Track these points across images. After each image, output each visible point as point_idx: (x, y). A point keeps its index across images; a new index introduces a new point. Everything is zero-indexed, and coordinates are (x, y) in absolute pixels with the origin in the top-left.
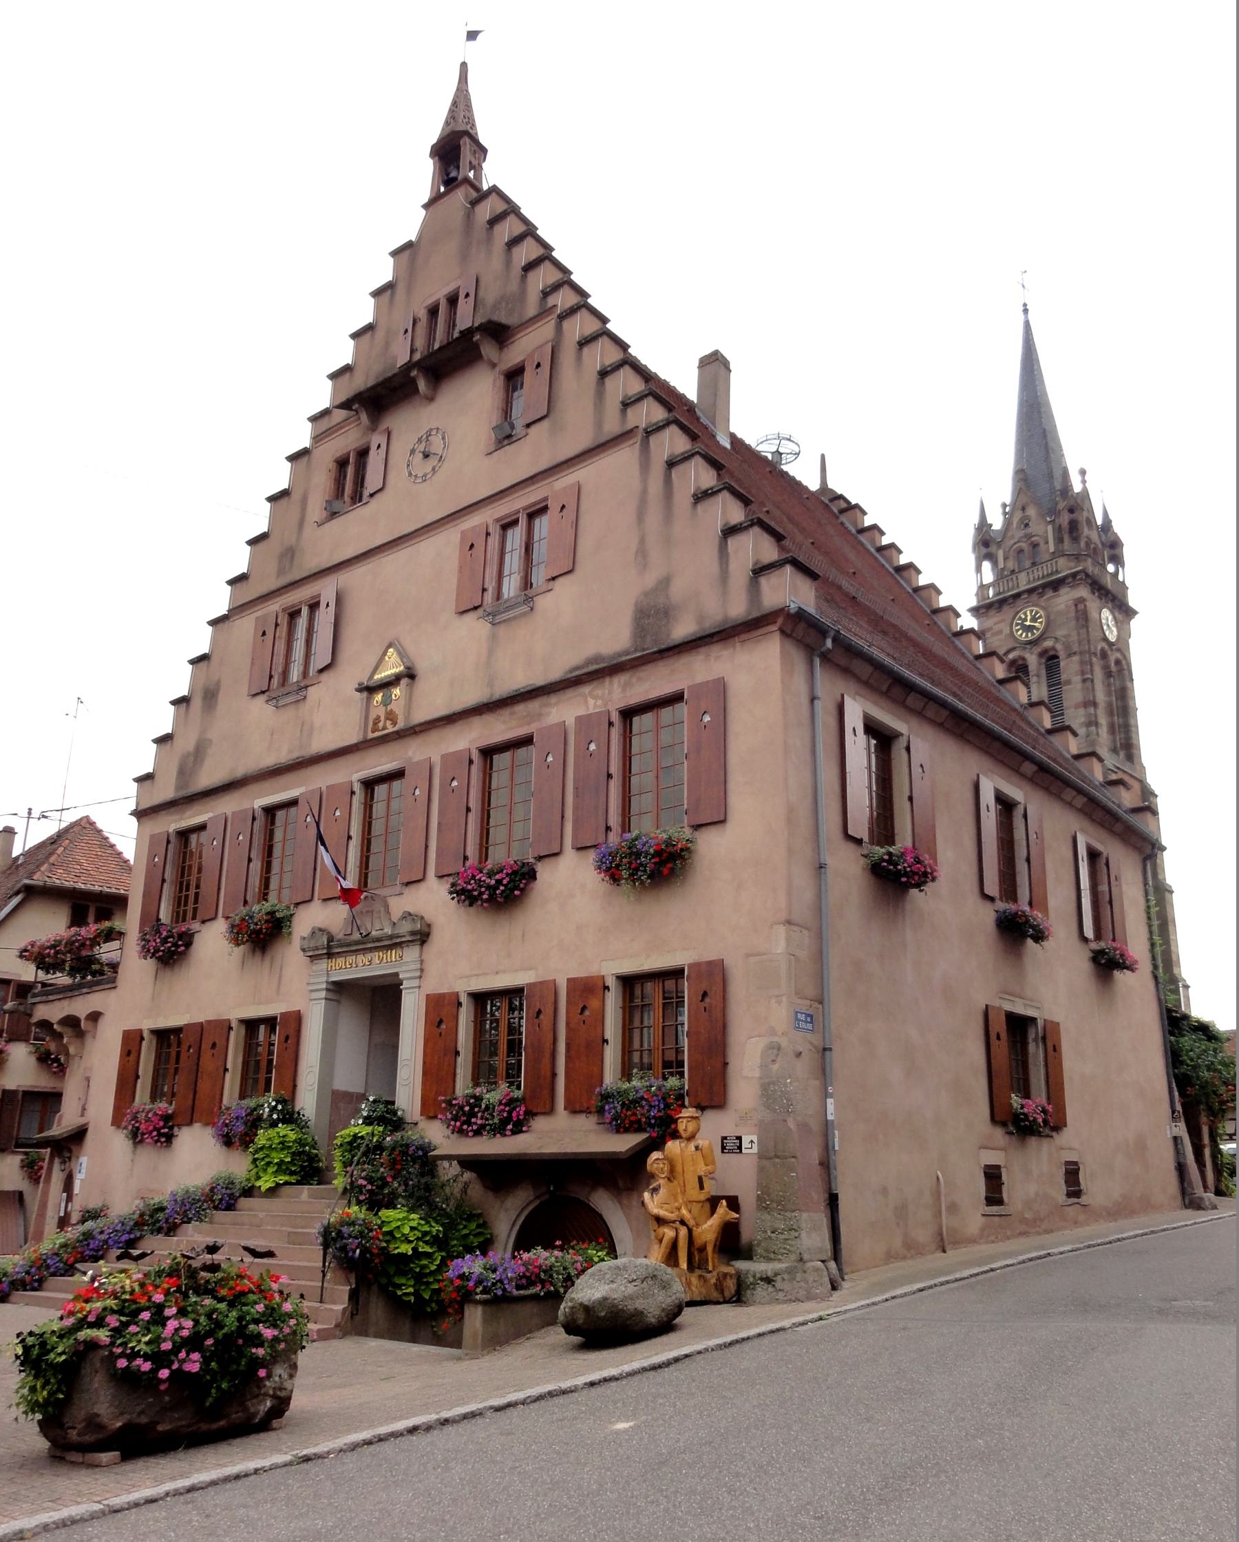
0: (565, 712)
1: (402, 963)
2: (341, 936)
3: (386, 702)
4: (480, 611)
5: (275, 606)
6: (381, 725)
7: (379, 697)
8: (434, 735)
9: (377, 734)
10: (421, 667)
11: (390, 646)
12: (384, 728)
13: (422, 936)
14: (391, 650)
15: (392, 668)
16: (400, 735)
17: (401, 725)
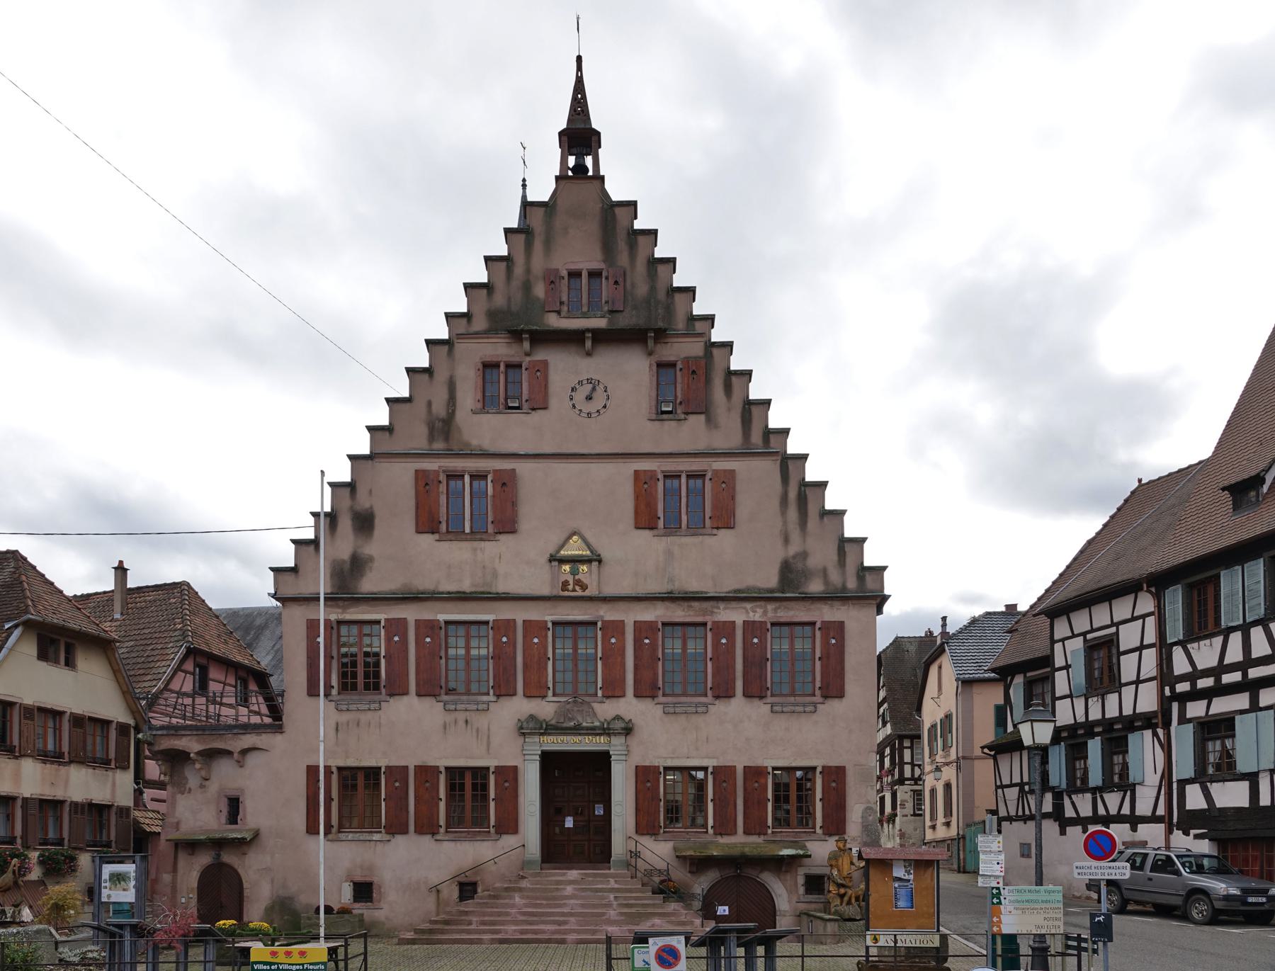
0: (737, 615)
1: (615, 746)
2: (553, 722)
3: (574, 572)
4: (655, 532)
5: (431, 465)
6: (570, 587)
7: (567, 568)
8: (622, 605)
9: (566, 594)
10: (605, 555)
11: (574, 534)
12: (574, 590)
13: (628, 731)
14: (575, 538)
15: (575, 548)
16: (591, 599)
17: (587, 593)
